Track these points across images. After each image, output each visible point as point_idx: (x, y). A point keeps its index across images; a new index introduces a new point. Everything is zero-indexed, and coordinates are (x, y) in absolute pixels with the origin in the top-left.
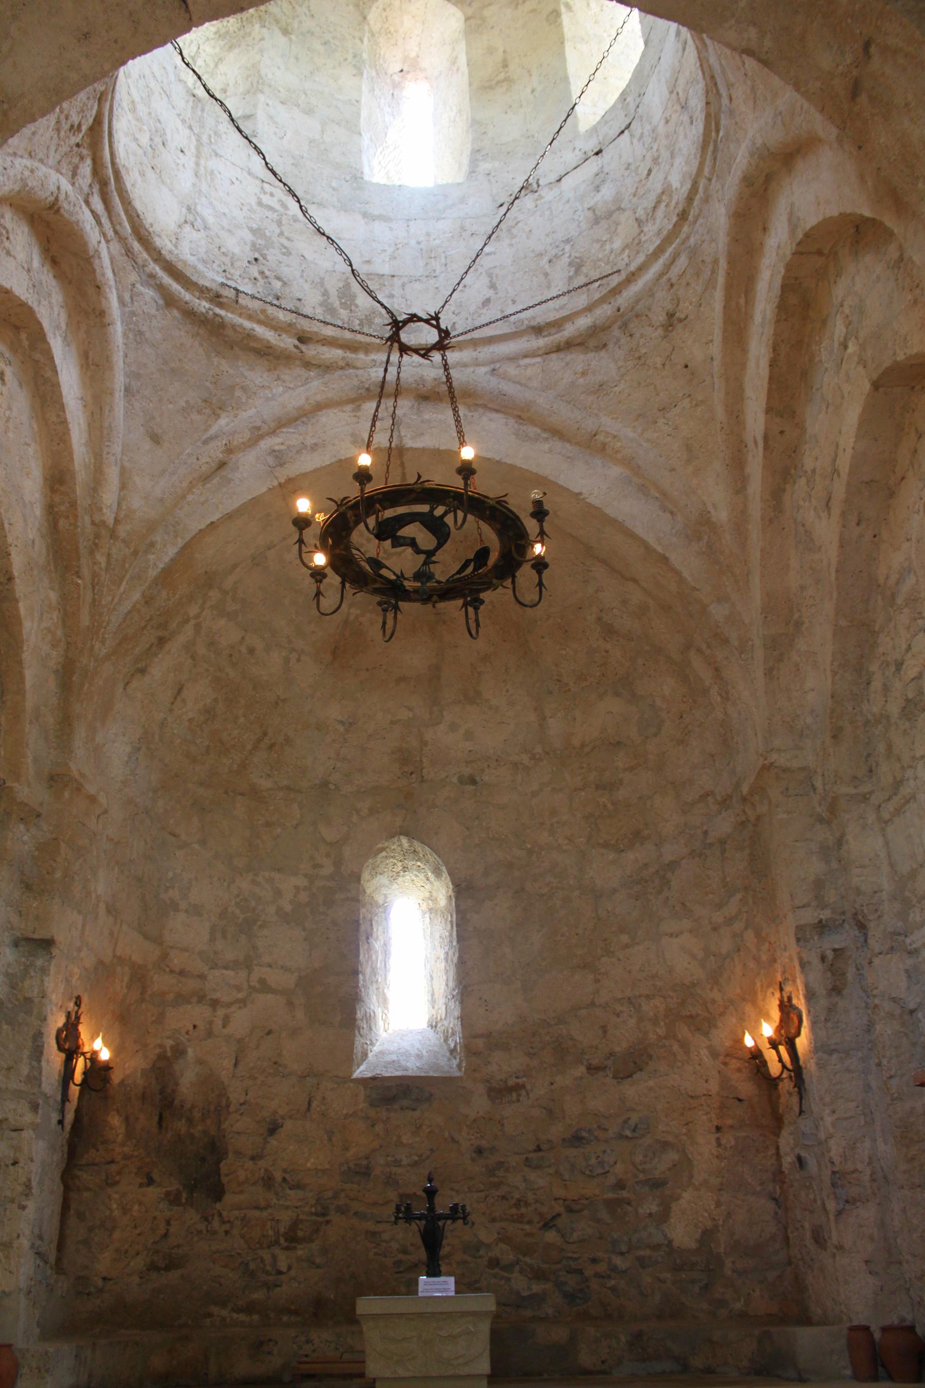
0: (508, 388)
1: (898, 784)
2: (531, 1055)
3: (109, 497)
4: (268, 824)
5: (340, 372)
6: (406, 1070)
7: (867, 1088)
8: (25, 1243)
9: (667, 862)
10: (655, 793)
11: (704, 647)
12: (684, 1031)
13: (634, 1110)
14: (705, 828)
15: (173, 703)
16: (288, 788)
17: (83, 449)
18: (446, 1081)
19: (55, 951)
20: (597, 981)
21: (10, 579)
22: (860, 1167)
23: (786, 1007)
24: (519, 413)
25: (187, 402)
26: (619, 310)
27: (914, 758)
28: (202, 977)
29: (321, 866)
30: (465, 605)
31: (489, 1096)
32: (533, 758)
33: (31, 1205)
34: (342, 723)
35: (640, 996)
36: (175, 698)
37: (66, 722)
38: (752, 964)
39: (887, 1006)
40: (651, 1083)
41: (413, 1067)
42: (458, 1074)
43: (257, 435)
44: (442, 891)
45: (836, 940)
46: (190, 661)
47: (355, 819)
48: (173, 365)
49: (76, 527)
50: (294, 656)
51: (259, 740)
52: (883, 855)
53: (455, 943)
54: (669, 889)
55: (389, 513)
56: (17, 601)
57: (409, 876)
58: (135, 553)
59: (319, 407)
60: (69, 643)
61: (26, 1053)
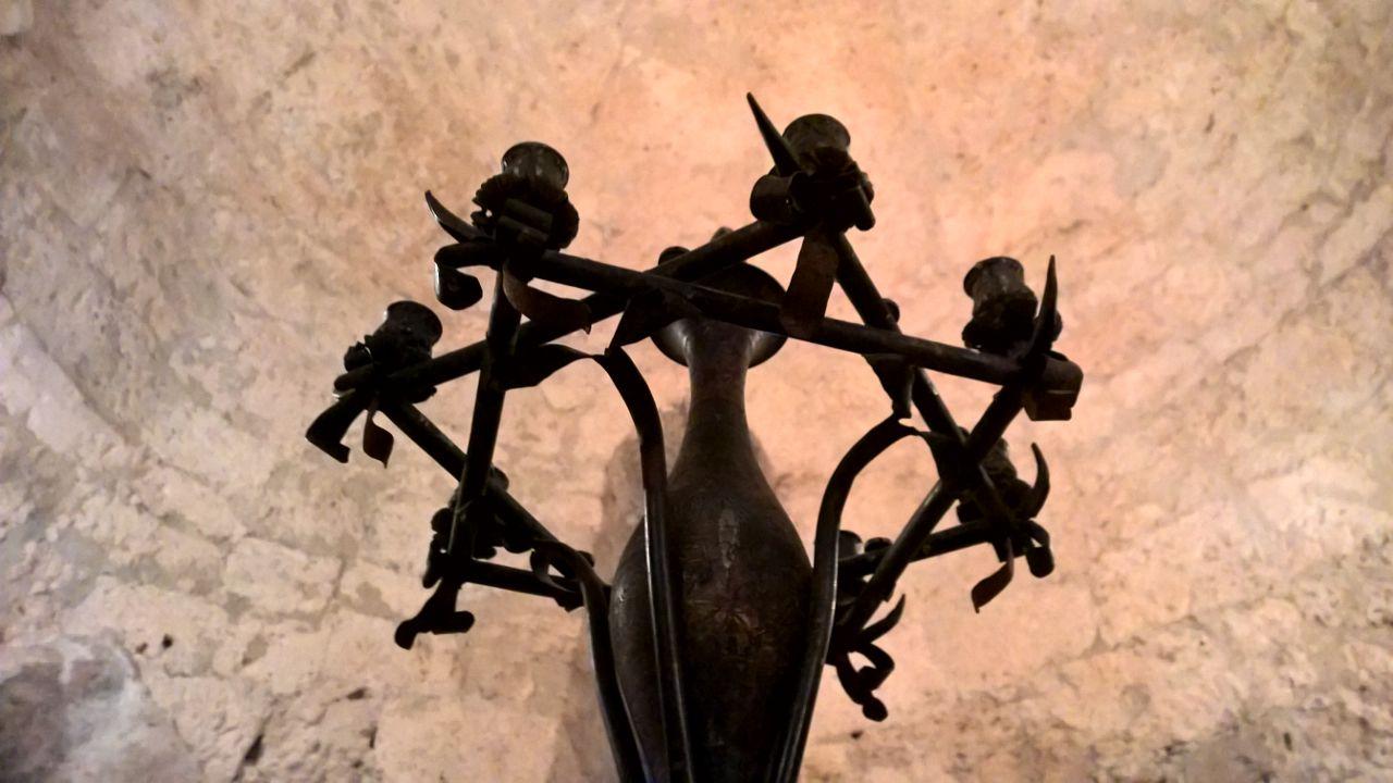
9: (1222, 357)
10: (1169, 267)
15: (288, 74)
20: (1098, 601)
28: (222, 541)
29: (537, 439)
32: (919, 284)
35: (1221, 609)
50: (526, 97)
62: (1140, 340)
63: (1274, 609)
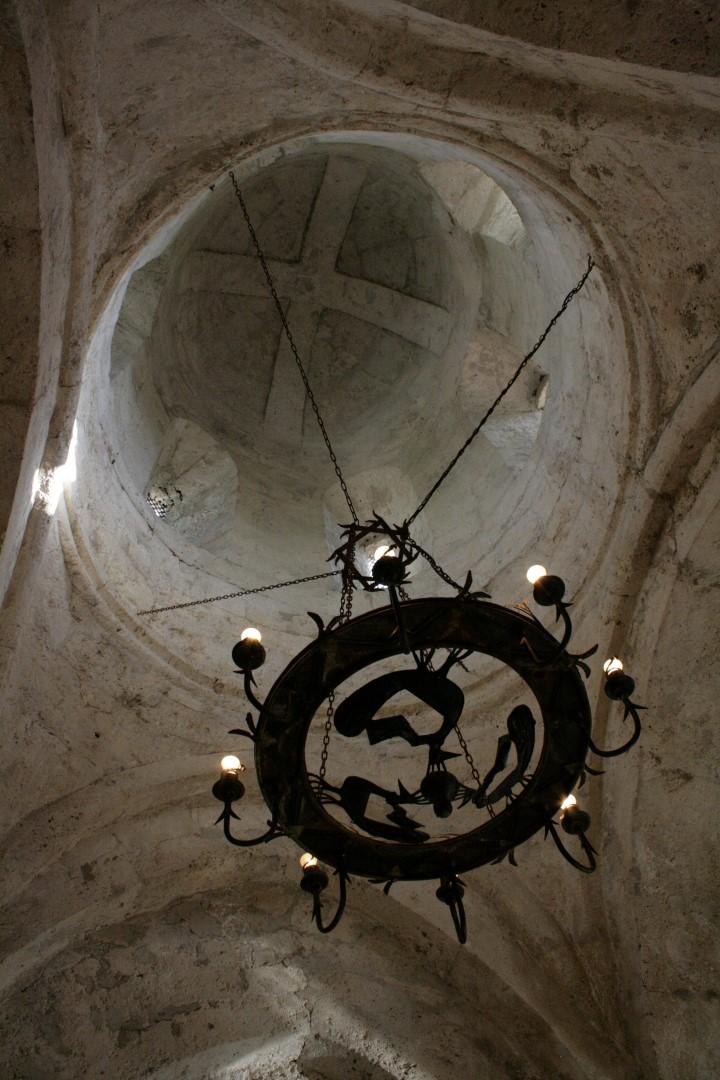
26: (118, 630)
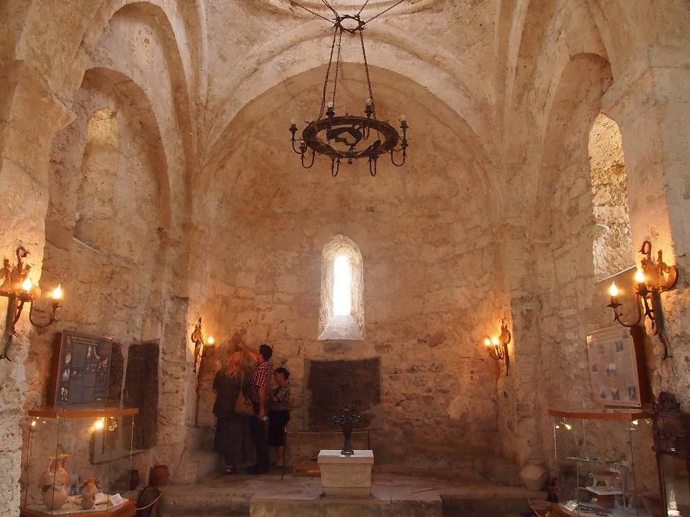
0: (393, 31)
1: (563, 243)
2: (394, 333)
3: (203, 91)
4: (280, 229)
5: (312, 21)
6: (340, 336)
7: (536, 371)
8: (182, 423)
11: (480, 161)
12: (461, 330)
13: (437, 360)
14: (475, 241)
16: (290, 213)
17: (190, 69)
18: (358, 342)
19: (190, 302)
20: (424, 303)
21: (160, 138)
22: (530, 403)
23: (504, 330)
24: (398, 44)
25: (238, 39)
27: (571, 234)
28: (252, 299)
30: (370, 161)
31: (375, 348)
33: (184, 408)
34: (313, 183)
36: (238, 177)
37: (189, 199)
38: (491, 306)
39: (548, 340)
40: (445, 350)
41: (343, 335)
42: (363, 339)
43: (272, 55)
44: (358, 258)
45: (529, 306)
46: (244, 160)
47: (319, 226)
48: (230, 22)
49: (188, 108)
51: (276, 192)
52: (553, 272)
53: (362, 282)
54: (458, 266)
55: (334, 128)
56: (163, 148)
57: (342, 249)
58: (217, 116)
59: (302, 40)
60: (188, 162)
61: (179, 346)
62: (445, 240)
63: (449, 315)
